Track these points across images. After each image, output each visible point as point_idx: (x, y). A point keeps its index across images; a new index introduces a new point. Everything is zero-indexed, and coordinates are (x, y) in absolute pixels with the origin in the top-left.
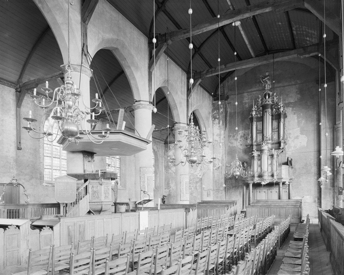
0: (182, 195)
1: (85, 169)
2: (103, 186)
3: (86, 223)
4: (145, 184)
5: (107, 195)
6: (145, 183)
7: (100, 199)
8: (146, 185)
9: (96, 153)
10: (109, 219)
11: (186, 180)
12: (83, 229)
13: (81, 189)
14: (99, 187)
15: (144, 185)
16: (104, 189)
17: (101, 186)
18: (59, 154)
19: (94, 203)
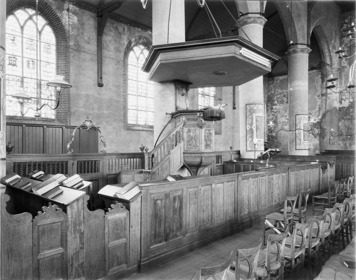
0: (298, 141)
1: (178, 105)
2: (203, 130)
3: (185, 193)
4: (253, 127)
5: (209, 143)
6: (252, 126)
7: (198, 148)
8: (254, 129)
9: (191, 83)
10: (221, 184)
11: (304, 122)
12: (179, 204)
13: (172, 134)
14: (197, 132)
15: (252, 129)
16: (205, 134)
17: (200, 129)
18: (145, 92)
19: (190, 155)
